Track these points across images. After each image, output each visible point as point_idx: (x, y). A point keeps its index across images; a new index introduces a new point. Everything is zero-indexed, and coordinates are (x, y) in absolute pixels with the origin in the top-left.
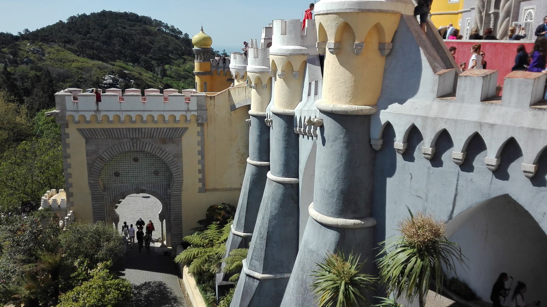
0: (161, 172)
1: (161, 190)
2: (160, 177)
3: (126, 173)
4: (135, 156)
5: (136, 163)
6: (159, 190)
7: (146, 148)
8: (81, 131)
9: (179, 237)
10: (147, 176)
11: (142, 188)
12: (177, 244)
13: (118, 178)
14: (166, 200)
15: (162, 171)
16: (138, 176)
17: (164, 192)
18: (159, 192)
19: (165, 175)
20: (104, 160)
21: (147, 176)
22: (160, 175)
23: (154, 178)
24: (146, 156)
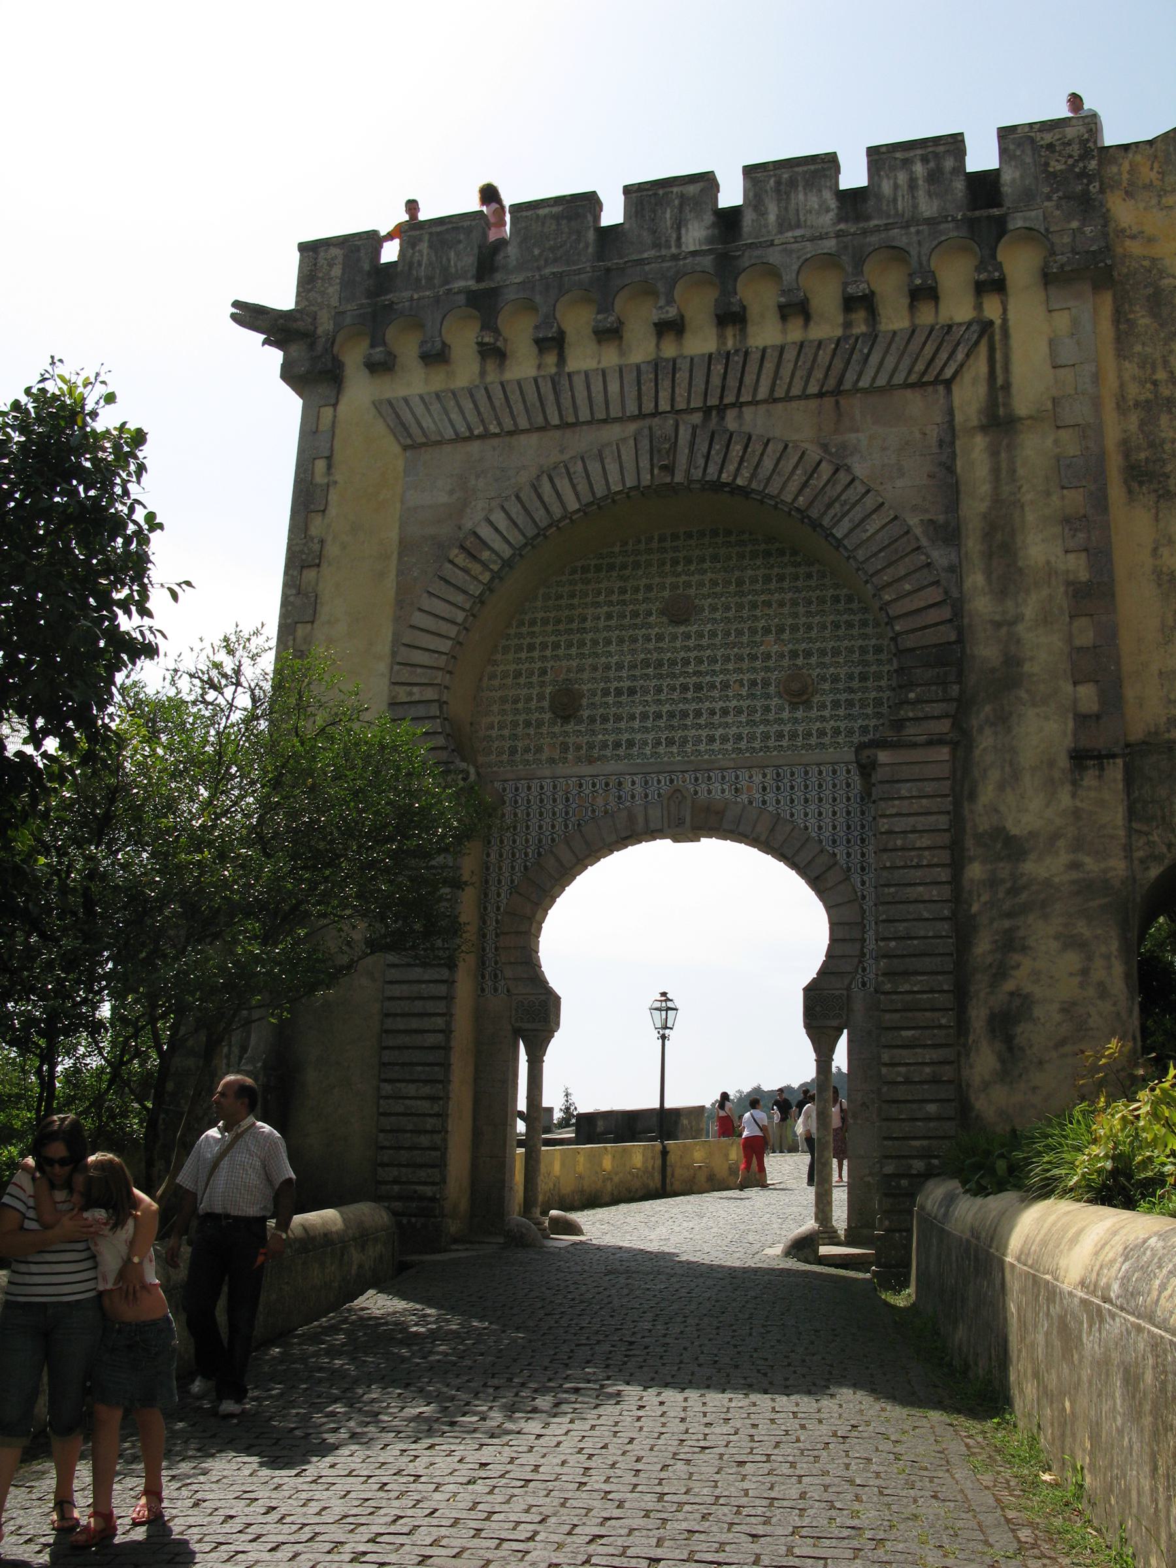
0: (827, 686)
1: (827, 809)
2: (823, 719)
3: (619, 693)
4: (674, 587)
5: (682, 629)
6: (812, 808)
7: (732, 468)
8: (389, 411)
9: (932, 1108)
10: (739, 711)
11: (703, 795)
12: (918, 1165)
13: (569, 728)
14: (856, 879)
15: (835, 679)
16: (684, 714)
17: (841, 819)
18: (812, 822)
19: (850, 704)
20: (485, 555)
21: (739, 711)
22: (823, 706)
23: (780, 721)
24: (740, 582)
